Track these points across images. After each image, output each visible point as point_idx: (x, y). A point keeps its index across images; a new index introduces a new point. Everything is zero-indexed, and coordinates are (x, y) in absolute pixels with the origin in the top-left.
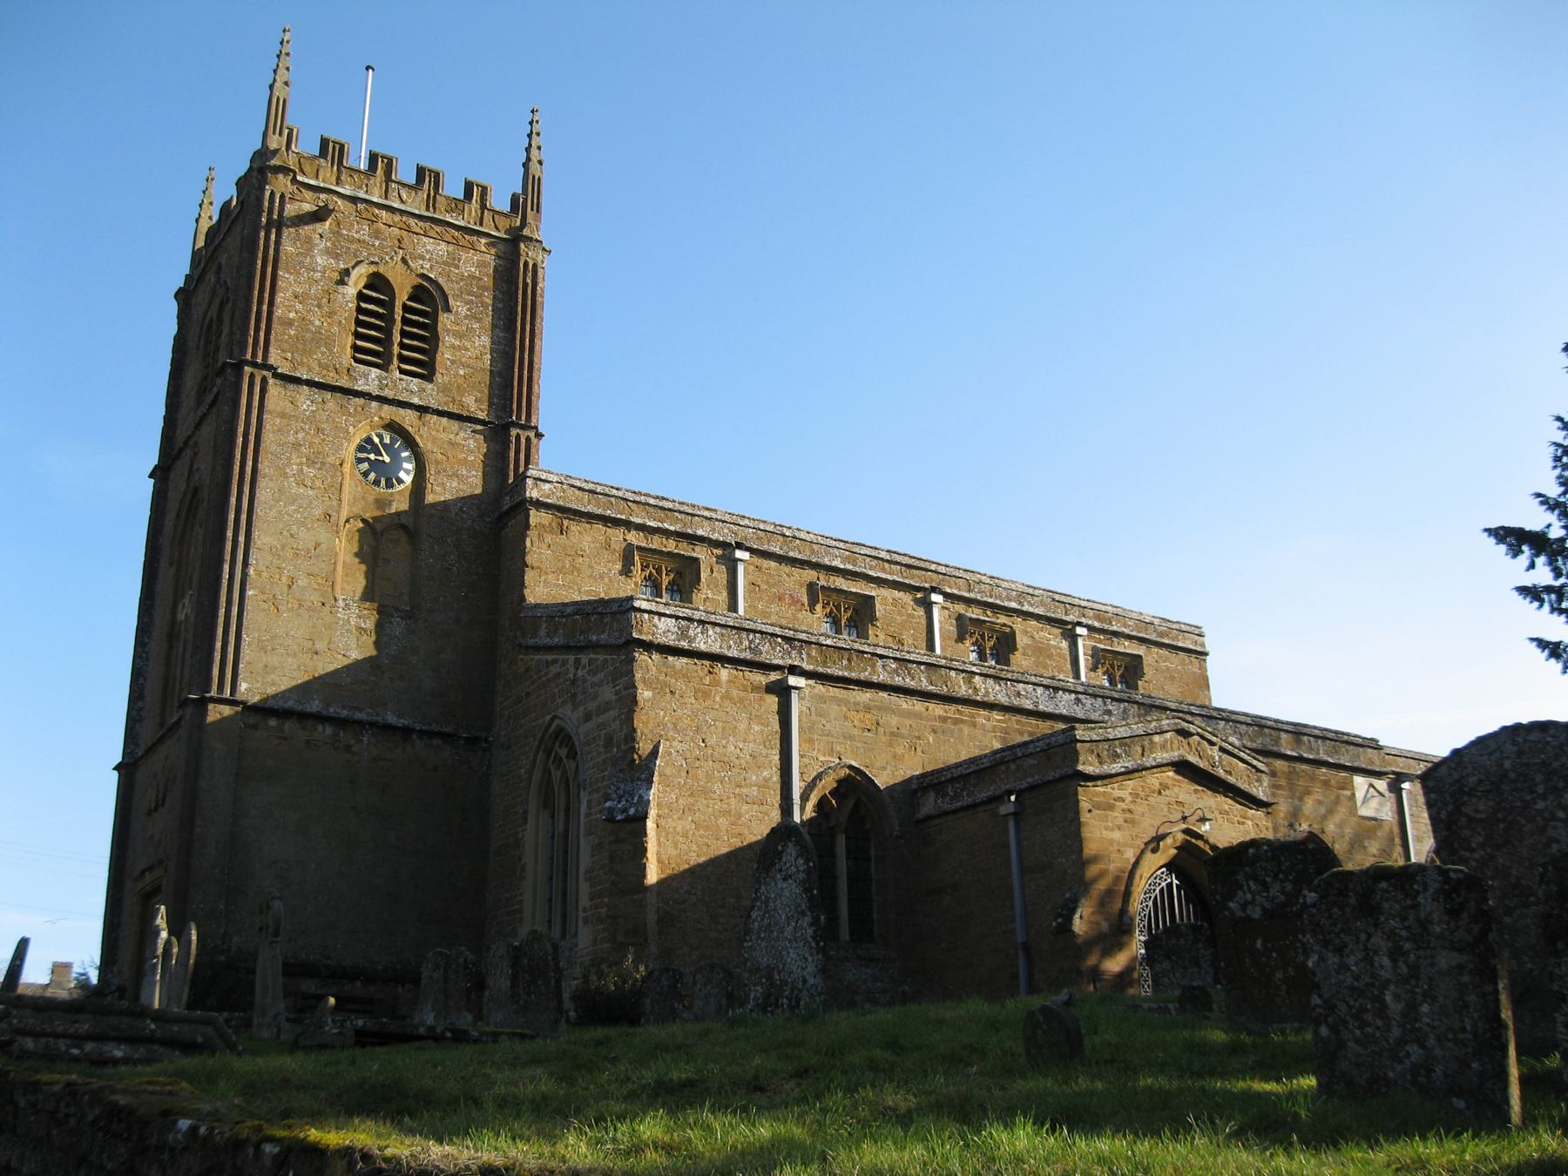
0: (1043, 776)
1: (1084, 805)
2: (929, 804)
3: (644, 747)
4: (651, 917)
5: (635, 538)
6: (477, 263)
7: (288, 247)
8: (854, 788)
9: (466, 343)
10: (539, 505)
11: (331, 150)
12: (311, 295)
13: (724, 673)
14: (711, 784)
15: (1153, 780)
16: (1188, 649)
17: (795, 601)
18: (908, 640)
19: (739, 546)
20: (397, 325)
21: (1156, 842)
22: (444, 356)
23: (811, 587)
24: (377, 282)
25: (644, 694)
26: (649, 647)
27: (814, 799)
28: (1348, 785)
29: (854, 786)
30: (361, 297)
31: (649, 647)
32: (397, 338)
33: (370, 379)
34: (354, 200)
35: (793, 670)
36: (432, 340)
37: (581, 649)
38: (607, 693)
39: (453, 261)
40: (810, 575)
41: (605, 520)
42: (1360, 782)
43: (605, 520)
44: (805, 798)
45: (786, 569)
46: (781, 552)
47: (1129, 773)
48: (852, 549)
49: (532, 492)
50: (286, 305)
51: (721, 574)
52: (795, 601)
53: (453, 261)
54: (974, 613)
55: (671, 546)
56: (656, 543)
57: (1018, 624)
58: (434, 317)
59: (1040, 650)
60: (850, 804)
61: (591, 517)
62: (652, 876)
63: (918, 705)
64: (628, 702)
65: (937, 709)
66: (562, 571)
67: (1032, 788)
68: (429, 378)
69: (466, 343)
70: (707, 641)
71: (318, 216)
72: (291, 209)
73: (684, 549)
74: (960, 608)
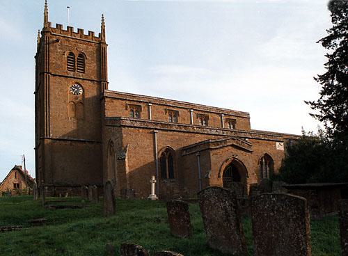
0: (203, 149)
1: (211, 154)
2: (184, 153)
3: (125, 146)
4: (127, 177)
5: (128, 102)
6: (92, 48)
7: (51, 48)
8: (168, 150)
9: (91, 66)
10: (107, 97)
11: (59, 26)
12: (58, 58)
13: (141, 130)
14: (138, 151)
15: (227, 149)
16: (245, 117)
17: (162, 112)
18: (186, 119)
19: (150, 103)
20: (77, 61)
21: (226, 161)
22: (87, 68)
23: (165, 110)
24: (71, 54)
25: (124, 135)
26: (124, 126)
27: (161, 153)
28: (275, 144)
29: (168, 150)
30: (68, 57)
31: (124, 126)
32: (76, 65)
33: (71, 74)
34: (64, 37)
35: (156, 129)
36: (84, 65)
37: (114, 126)
38: (118, 135)
39: (87, 48)
40: (165, 107)
41: (121, 99)
42: (277, 143)
43: (121, 99)
44: (158, 153)
45: (160, 106)
46: (158, 102)
47: (221, 148)
48: (175, 102)
49: (105, 95)
50: (52, 60)
51: (147, 108)
52: (162, 112)
53: (87, 48)
54: (200, 113)
55: (135, 103)
56: (132, 103)
57: (209, 114)
58: (84, 60)
59: (214, 119)
60: (168, 153)
61: (118, 99)
62: (128, 170)
63: (183, 134)
64: (122, 138)
65: (187, 134)
66: (111, 111)
67: (202, 151)
68: (84, 73)
69: (91, 66)
70: (137, 124)
71: (57, 41)
72: (51, 40)
73: (138, 104)
74: (197, 112)
